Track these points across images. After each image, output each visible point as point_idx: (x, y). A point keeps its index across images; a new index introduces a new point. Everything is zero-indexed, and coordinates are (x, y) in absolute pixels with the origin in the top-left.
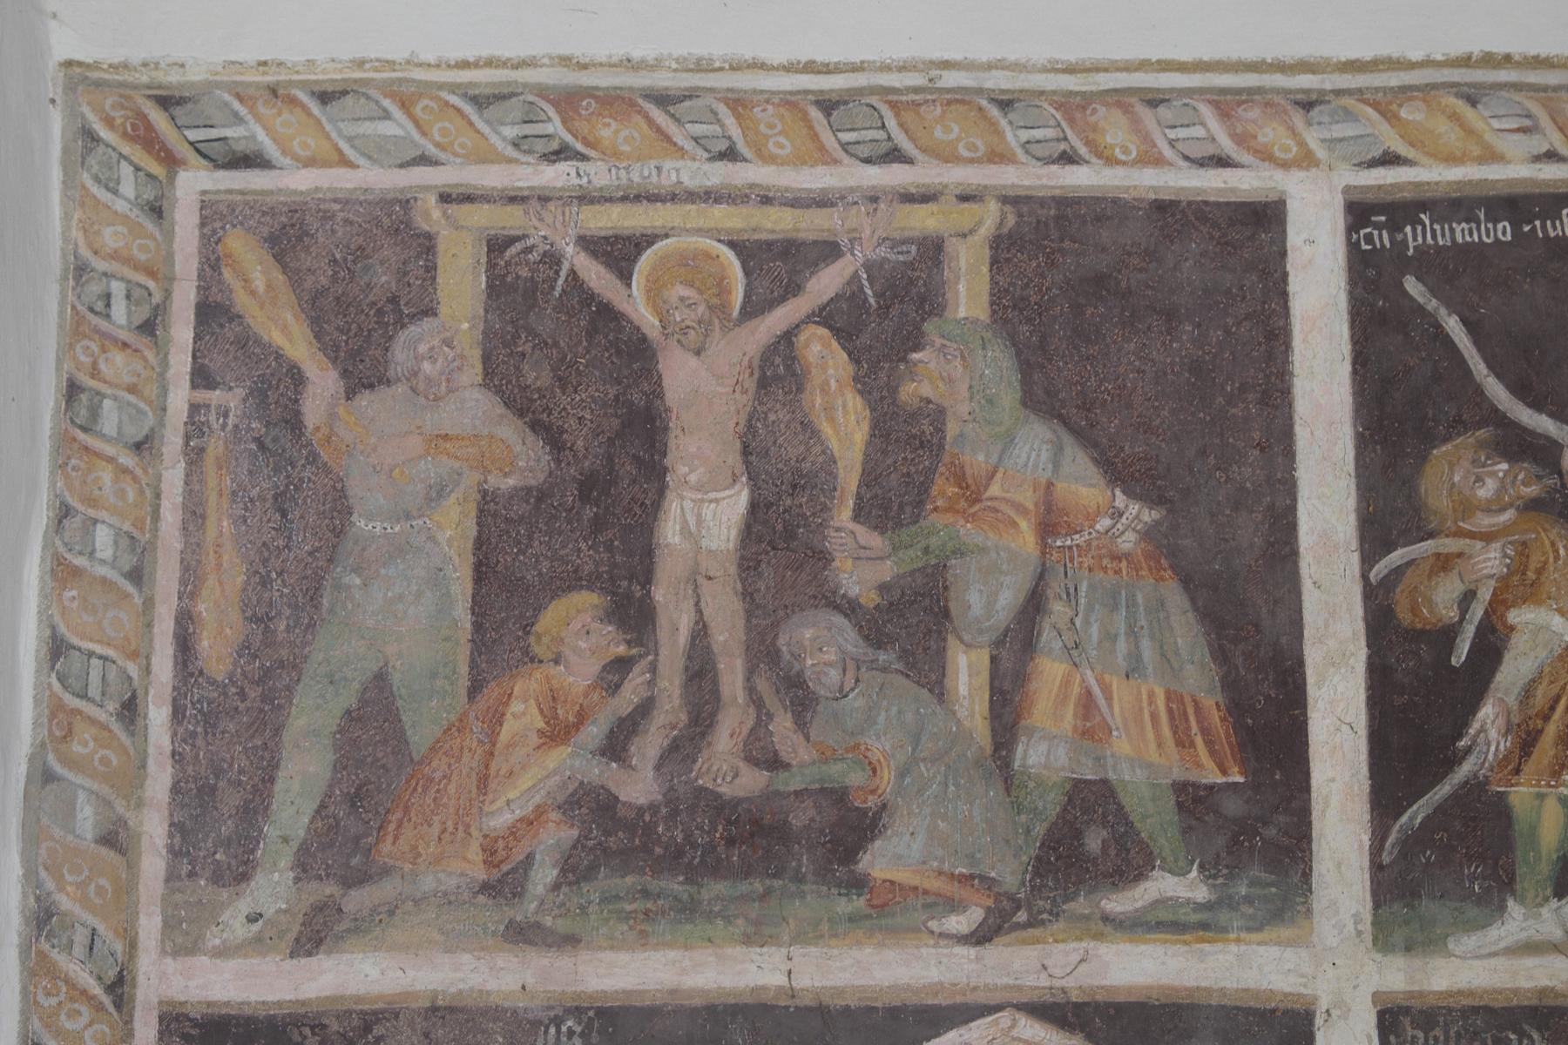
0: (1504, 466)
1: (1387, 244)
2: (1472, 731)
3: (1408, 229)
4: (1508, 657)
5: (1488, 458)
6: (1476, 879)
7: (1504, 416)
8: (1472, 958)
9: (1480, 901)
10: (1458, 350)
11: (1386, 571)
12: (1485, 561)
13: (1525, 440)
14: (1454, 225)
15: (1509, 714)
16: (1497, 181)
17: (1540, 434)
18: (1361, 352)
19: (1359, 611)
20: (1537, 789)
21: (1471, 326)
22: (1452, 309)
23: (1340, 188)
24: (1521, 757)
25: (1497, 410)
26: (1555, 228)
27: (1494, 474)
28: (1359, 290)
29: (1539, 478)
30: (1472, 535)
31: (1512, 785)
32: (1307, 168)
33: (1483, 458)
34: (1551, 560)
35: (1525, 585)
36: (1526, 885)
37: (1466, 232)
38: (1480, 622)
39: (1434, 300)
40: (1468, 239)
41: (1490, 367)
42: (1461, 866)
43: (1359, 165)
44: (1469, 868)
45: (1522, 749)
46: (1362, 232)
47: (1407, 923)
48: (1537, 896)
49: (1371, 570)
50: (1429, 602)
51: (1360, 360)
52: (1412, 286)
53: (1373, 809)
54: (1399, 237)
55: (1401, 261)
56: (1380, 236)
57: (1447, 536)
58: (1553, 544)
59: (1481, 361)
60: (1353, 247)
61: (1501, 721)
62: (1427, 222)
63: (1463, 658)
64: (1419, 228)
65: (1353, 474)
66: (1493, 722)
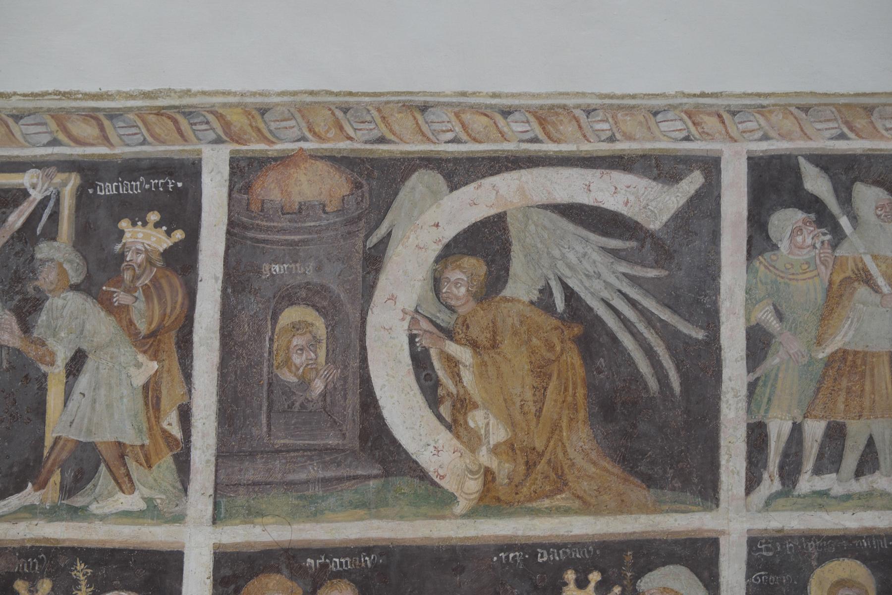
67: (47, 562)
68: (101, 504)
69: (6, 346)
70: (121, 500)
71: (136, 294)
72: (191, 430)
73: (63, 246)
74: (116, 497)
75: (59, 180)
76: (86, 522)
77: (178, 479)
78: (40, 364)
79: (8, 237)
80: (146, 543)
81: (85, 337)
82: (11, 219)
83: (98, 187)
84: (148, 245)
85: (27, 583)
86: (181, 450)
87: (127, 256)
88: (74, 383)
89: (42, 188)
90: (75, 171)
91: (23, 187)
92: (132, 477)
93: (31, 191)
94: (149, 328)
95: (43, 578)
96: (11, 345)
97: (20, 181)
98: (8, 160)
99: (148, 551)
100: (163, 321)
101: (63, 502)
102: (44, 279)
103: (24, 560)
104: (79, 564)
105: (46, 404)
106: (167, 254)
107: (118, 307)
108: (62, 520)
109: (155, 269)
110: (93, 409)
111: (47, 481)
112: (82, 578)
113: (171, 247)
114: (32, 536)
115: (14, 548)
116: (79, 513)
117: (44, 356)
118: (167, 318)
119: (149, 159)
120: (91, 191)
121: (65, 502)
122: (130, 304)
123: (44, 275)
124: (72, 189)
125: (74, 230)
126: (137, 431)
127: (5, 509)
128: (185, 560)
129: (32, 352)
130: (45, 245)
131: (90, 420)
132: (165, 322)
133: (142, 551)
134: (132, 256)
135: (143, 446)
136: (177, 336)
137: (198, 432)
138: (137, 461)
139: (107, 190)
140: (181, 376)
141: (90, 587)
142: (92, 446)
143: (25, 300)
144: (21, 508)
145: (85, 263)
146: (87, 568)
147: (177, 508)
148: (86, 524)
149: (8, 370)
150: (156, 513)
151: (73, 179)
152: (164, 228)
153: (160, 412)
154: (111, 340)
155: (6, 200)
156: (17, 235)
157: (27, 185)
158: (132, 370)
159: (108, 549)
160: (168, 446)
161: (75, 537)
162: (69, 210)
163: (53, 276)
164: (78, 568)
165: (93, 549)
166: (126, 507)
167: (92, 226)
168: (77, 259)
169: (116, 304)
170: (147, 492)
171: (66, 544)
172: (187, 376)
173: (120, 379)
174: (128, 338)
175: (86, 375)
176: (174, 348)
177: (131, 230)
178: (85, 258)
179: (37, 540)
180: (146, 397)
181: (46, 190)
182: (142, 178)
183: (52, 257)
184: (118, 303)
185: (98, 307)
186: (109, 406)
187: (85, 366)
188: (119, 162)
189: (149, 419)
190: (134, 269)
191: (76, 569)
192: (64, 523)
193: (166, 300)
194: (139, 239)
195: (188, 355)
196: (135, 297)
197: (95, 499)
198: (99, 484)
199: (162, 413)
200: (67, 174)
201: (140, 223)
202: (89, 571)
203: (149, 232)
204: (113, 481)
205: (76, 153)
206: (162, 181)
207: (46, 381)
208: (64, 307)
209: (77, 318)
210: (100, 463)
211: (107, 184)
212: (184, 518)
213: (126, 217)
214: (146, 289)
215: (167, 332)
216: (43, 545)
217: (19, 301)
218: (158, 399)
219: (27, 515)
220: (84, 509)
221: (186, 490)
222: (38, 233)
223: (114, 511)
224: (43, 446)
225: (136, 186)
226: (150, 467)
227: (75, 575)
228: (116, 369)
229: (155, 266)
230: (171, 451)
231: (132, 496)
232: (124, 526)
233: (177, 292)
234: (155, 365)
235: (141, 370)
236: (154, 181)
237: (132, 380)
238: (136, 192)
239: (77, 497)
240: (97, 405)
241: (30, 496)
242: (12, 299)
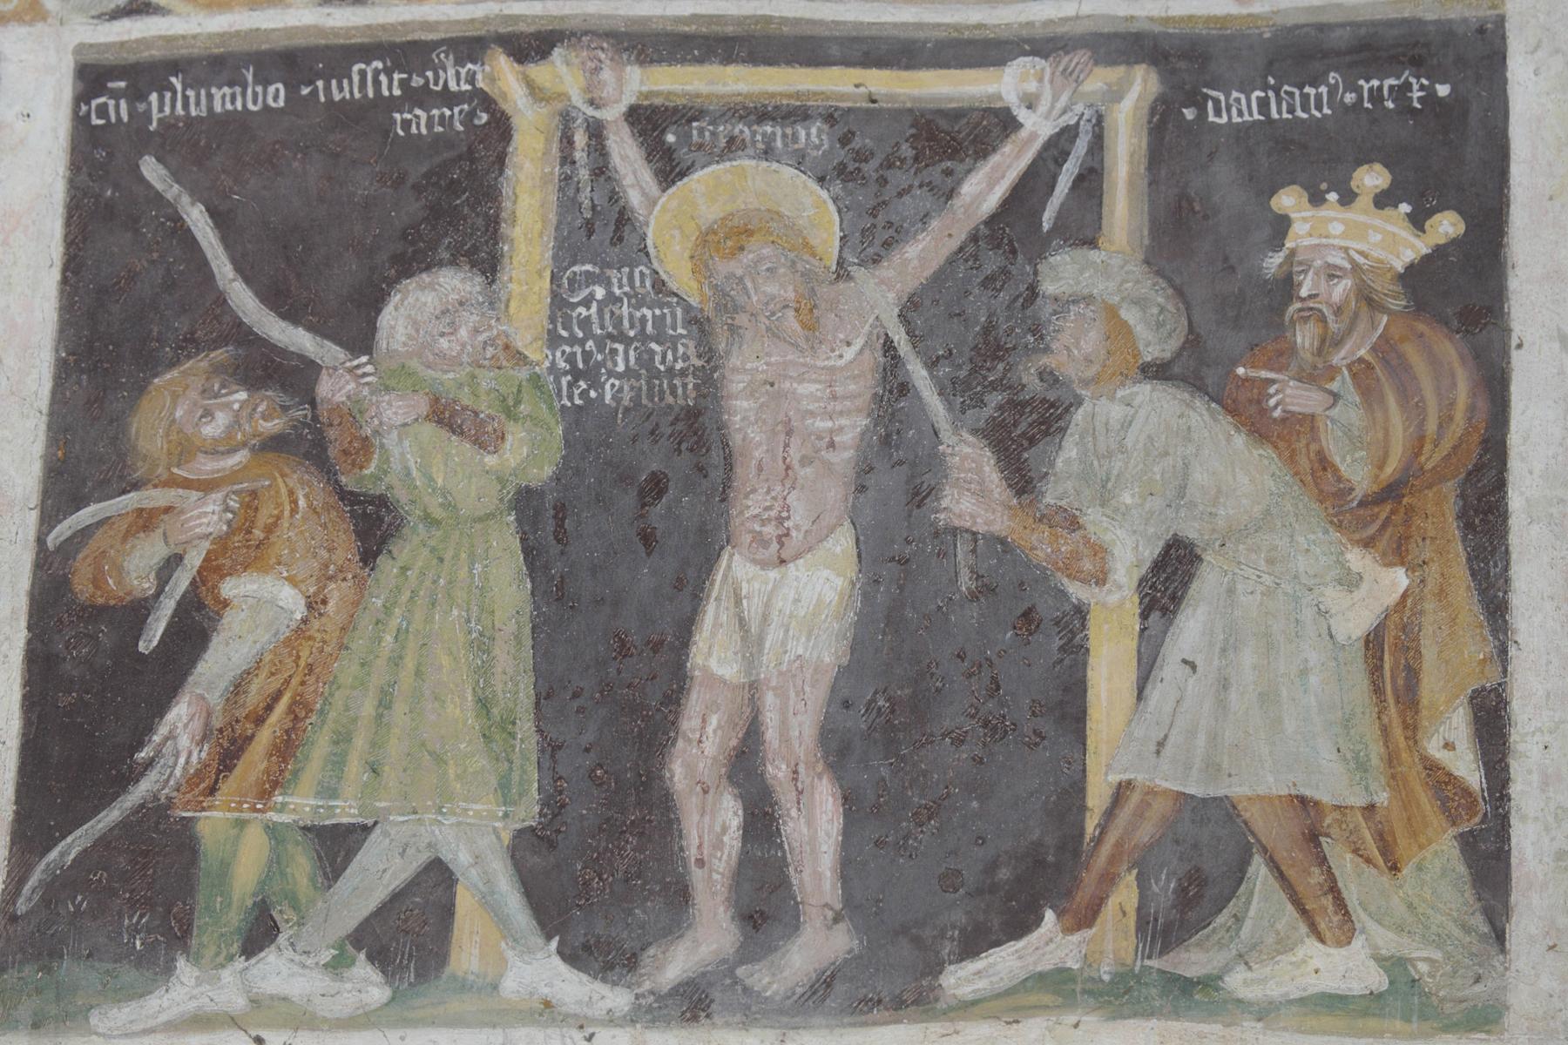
0: (242, 395)
1: (125, 118)
2: (156, 738)
3: (154, 97)
4: (216, 641)
5: (223, 386)
6: (138, 932)
7: (250, 331)
8: (120, 1036)
9: (141, 961)
10: (200, 250)
11: (69, 533)
12: (199, 517)
13: (273, 361)
14: (214, 90)
15: (209, 715)
16: (274, 30)
17: (293, 353)
18: (76, 256)
19: (25, 583)
20: (236, 815)
21: (220, 218)
22: (197, 195)
23: (71, 47)
24: (219, 772)
25: (241, 324)
26: (341, 89)
27: (228, 405)
28: (84, 177)
29: (285, 409)
30: (187, 484)
31: (203, 809)
32: (31, 23)
33: (216, 387)
34: (287, 513)
35: (248, 547)
36: (205, 939)
37: (228, 99)
38: (183, 596)
39: (176, 186)
40: (229, 106)
41: (239, 269)
42: (121, 916)
43: (99, 17)
44: (131, 918)
45: (222, 761)
46: (94, 103)
47: (39, 991)
48: (217, 954)
49: (49, 532)
50: (119, 570)
51: (73, 266)
52: (151, 169)
53: (13, 843)
54: (141, 107)
55: (140, 138)
56: (117, 107)
57: (155, 486)
58: (291, 493)
59: (227, 262)
60: (80, 122)
61: (197, 725)
62: (179, 87)
63: (155, 643)
64: (168, 95)
65: (45, 410)
66: (186, 726)
68: (1260, 971)
69: (967, 531)
71: (1334, 386)
72: (1507, 766)
73: (1116, 261)
74: (1300, 952)
75: (1100, 84)
76: (1215, 1022)
77: (1478, 905)
78: (1065, 581)
79: (961, 236)
81: (1192, 505)
82: (969, 188)
83: (1210, 104)
84: (1361, 253)
86: (1482, 822)
87: (1300, 285)
88: (1165, 633)
89: (1052, 107)
90: (1143, 61)
91: (998, 105)
92: (1345, 894)
93: (1022, 115)
94: (1377, 476)
96: (981, 528)
97: (991, 89)
98: (955, 35)
100: (1417, 454)
102: (1067, 348)
105: (1085, 691)
106: (1415, 277)
107: (1284, 420)
109: (1385, 319)
110: (1222, 705)
111: (1100, 906)
113: (1426, 259)
116: (1197, 997)
117: (1076, 556)
118: (1428, 447)
119: (1352, 24)
120: (1189, 114)
122: (1319, 411)
123: (1066, 338)
124: (1136, 108)
125: (1146, 217)
126: (1352, 765)
129: (1041, 546)
130: (1068, 259)
131: (1213, 738)
132: (1423, 459)
134: (1316, 284)
135: (1370, 809)
136: (1462, 496)
137: (1530, 772)
138: (1356, 851)
139: (1234, 111)
140: (1477, 608)
142: (1225, 809)
143: (1016, 407)
145: (1181, 305)
147: (1478, 988)
148: (1217, 1028)
149: (973, 597)
151: (1139, 80)
152: (1405, 208)
153: (1417, 713)
154: (1267, 512)
155: (953, 139)
156: (987, 232)
157: (1011, 98)
158: (1332, 596)
160: (1445, 809)
162: (1131, 163)
163: (1091, 341)
166: (1329, 983)
167: (1197, 208)
168: (1160, 297)
169: (1277, 413)
170: (1388, 941)
172: (1496, 610)
173: (1297, 620)
174: (1315, 505)
175: (1199, 611)
176: (1454, 528)
177: (1309, 214)
178: (1180, 292)
180: (1375, 670)
181: (1064, 112)
182: (1333, 77)
183: (1086, 292)
184: (1284, 411)
185: (1226, 421)
186: (1268, 698)
187: (1195, 586)
188: (1267, 35)
189: (1385, 731)
190: (1323, 319)
193: (1422, 400)
194: (1335, 237)
195: (1494, 549)
196: (1331, 393)
197: (1241, 956)
198: (1252, 913)
199: (1424, 713)
200: (1120, 70)
201: (1333, 197)
203: (1362, 218)
204: (1289, 907)
205: (1143, 13)
206: (1392, 81)
207: (1084, 626)
208: (1126, 424)
209: (1167, 454)
210: (1251, 856)
211: (1235, 94)
212: (1501, 1015)
213: (1293, 183)
214: (1361, 372)
215: (1430, 487)
217: (1000, 408)
218: (1412, 674)
220: (1209, 983)
222: (1046, 226)
223: (1295, 995)
224: (1083, 808)
225: (1319, 97)
226: (1394, 868)
228: (1286, 594)
229: (1383, 309)
230: (1454, 824)
231: (1343, 951)
233: (1453, 375)
234: (1400, 579)
235: (1357, 595)
236: (1367, 81)
237: (1332, 621)
238: (1318, 115)
240: (1233, 695)
242: (981, 403)
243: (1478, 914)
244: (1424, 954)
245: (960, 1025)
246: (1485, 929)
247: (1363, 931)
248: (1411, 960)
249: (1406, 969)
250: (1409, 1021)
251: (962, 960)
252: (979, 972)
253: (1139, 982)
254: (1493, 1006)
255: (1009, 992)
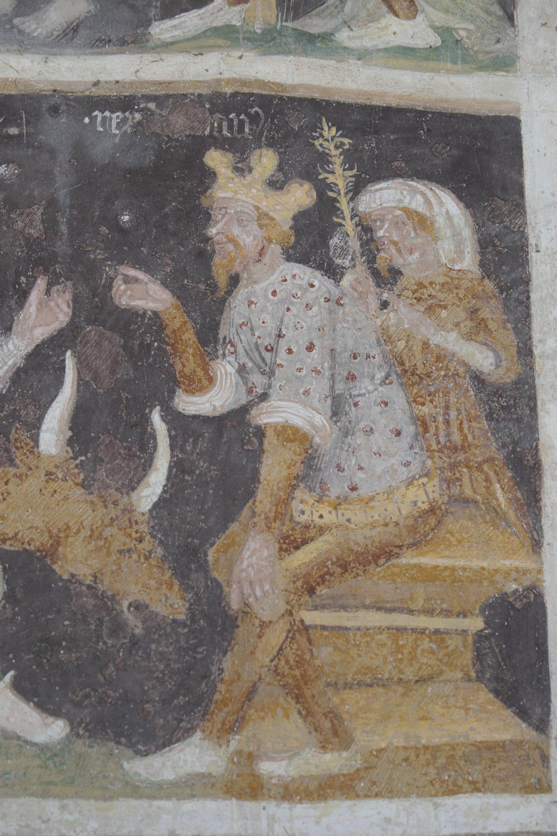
67: (266, 121)
70: (394, 28)
74: (383, 22)
76: (331, 59)
80: (447, 101)
85: (230, 155)
95: (260, 147)
99: (452, 116)
101: (285, 24)
103: (221, 116)
104: (326, 128)
108: (288, 52)
112: (334, 152)
114: (234, 75)
115: (200, 95)
116: (318, 44)
121: (290, 24)
127: (177, 33)
128: (524, 131)
133: (440, 114)
141: (351, 168)
144: (206, 31)
146: (341, 136)
147: (498, 46)
148: (332, 62)
150: (459, 51)
159: (379, 107)
161: (315, 83)
164: (326, 134)
165: (350, 106)
170: (440, 18)
171: (300, 94)
179: (244, 83)
191: (321, 135)
192: (291, 58)
202: (346, 141)
212: (514, 62)
216: (255, 91)
219: (220, 42)
221: (511, 18)
223: (382, 46)
227: (321, 145)
231: (411, 22)
232: (403, 72)
239: (310, 18)
241: (222, 13)
243: (495, 5)
244: (463, 26)
245: (164, 56)
246: (500, 13)
247: (423, 11)
248: (455, 29)
249: (452, 34)
250: (456, 63)
251: (163, 19)
252: (175, 26)
253: (280, 34)
254: (509, 57)
255: (194, 38)
